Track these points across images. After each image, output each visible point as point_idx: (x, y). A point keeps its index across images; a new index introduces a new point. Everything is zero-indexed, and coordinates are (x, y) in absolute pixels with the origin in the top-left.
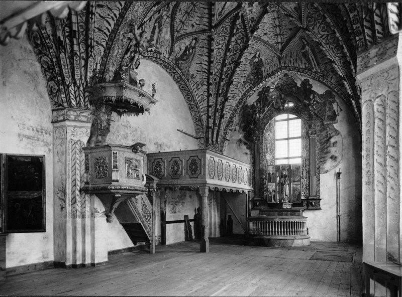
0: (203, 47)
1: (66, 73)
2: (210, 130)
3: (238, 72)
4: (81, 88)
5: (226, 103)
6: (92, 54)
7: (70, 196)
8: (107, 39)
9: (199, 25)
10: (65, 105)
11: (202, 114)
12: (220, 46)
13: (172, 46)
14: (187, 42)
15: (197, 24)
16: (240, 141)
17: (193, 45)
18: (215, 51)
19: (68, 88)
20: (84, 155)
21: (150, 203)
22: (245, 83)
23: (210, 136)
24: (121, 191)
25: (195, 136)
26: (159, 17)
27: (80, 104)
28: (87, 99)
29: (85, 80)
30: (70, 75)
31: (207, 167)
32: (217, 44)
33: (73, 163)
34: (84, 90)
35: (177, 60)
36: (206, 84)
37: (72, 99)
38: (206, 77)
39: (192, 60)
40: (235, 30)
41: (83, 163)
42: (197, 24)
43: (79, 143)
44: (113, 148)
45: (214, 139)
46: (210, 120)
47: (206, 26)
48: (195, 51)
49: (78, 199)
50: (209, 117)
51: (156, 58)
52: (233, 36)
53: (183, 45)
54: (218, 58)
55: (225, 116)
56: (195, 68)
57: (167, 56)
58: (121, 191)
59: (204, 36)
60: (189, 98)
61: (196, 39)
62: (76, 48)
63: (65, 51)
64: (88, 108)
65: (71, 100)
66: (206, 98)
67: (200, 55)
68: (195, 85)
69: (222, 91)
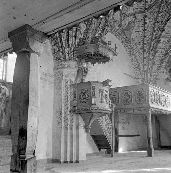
0: (140, 22)
2: (145, 73)
3: (163, 35)
4: (72, 49)
5: (156, 55)
6: (80, 29)
7: (64, 115)
9: (138, 8)
10: (62, 59)
11: (140, 63)
12: (151, 20)
13: (121, 22)
14: (130, 19)
15: (136, 8)
16: (167, 79)
17: (133, 21)
18: (148, 23)
19: (65, 49)
20: (72, 89)
21: (110, 122)
22: (168, 41)
24: (97, 111)
25: (135, 77)
27: (71, 58)
28: (75, 55)
29: (75, 44)
30: (66, 41)
32: (149, 19)
33: (66, 94)
34: (73, 50)
35: (123, 30)
36: (142, 43)
38: (142, 40)
39: (133, 29)
40: (161, 10)
41: (72, 94)
42: (136, 8)
43: (70, 81)
44: (92, 83)
46: (145, 66)
47: (143, 9)
48: (135, 24)
49: (69, 117)
50: (144, 64)
51: (112, 30)
52: (160, 13)
53: (127, 21)
54: (149, 27)
55: (156, 63)
56: (135, 34)
57: (118, 28)
58: (97, 111)
60: (131, 53)
61: (135, 17)
66: (142, 52)
67: (138, 26)
68: (135, 45)
69: (153, 48)
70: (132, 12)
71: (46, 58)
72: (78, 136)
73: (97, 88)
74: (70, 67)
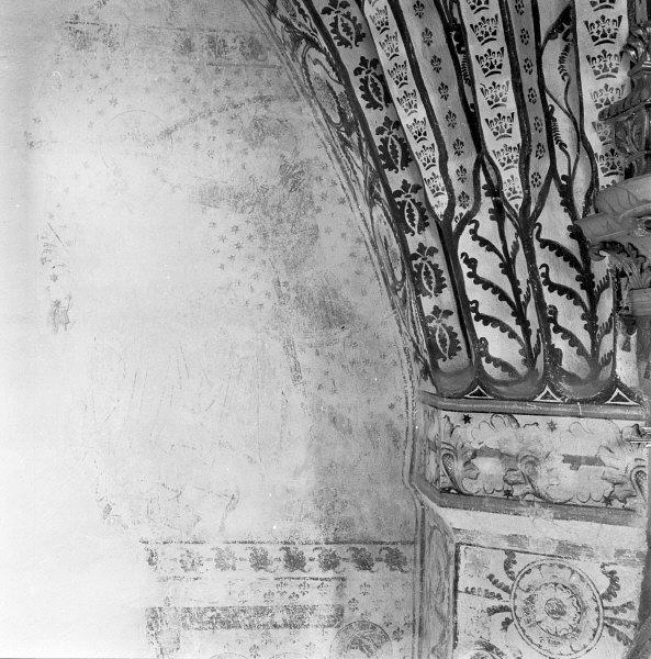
1: (420, 136)
19: (449, 241)
37: (487, 320)
64: (615, 383)
65: (481, 330)
71: (296, 368)
74: (541, 484)
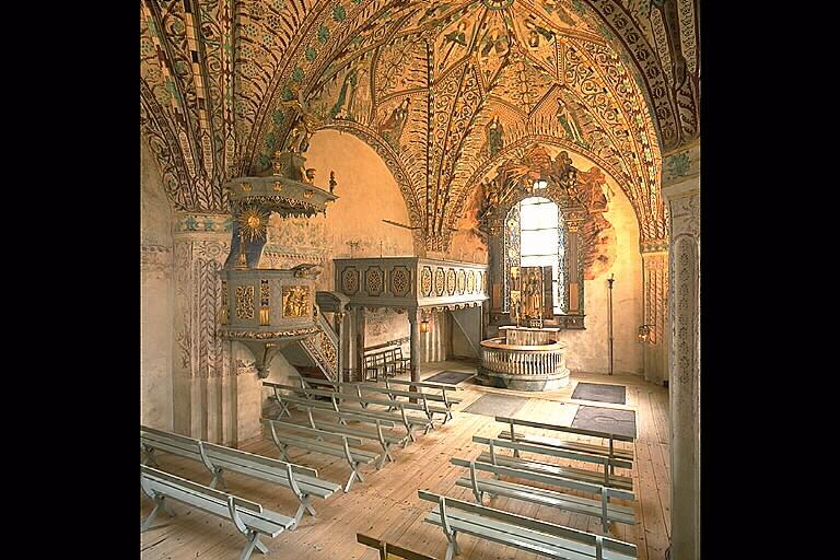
4: (217, 183)
8: (256, 110)
12: (442, 109)
19: (195, 183)
23: (430, 226)
26: (352, 72)
31: (419, 282)
35: (380, 127)
43: (212, 263)
45: (436, 230)
50: (428, 201)
57: (366, 124)
59: (420, 98)
61: (408, 99)
62: (204, 123)
63: (187, 129)
70: (400, 88)
72: (234, 391)
73: (276, 285)
